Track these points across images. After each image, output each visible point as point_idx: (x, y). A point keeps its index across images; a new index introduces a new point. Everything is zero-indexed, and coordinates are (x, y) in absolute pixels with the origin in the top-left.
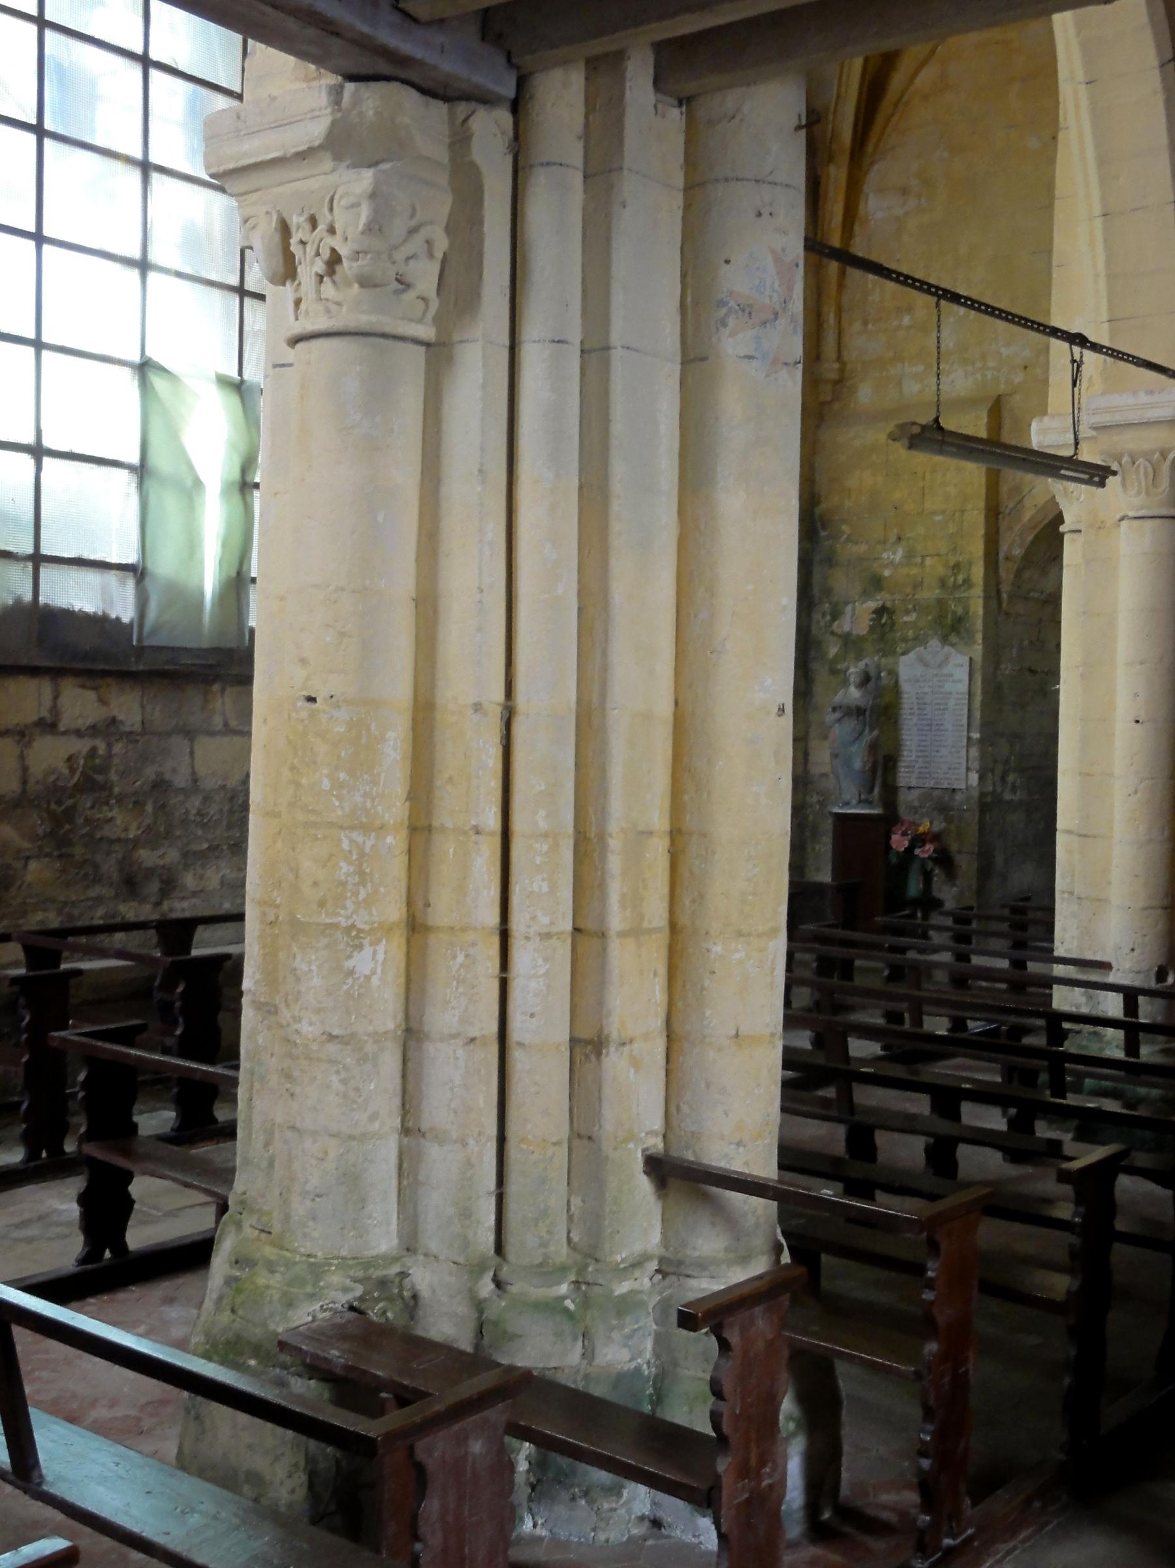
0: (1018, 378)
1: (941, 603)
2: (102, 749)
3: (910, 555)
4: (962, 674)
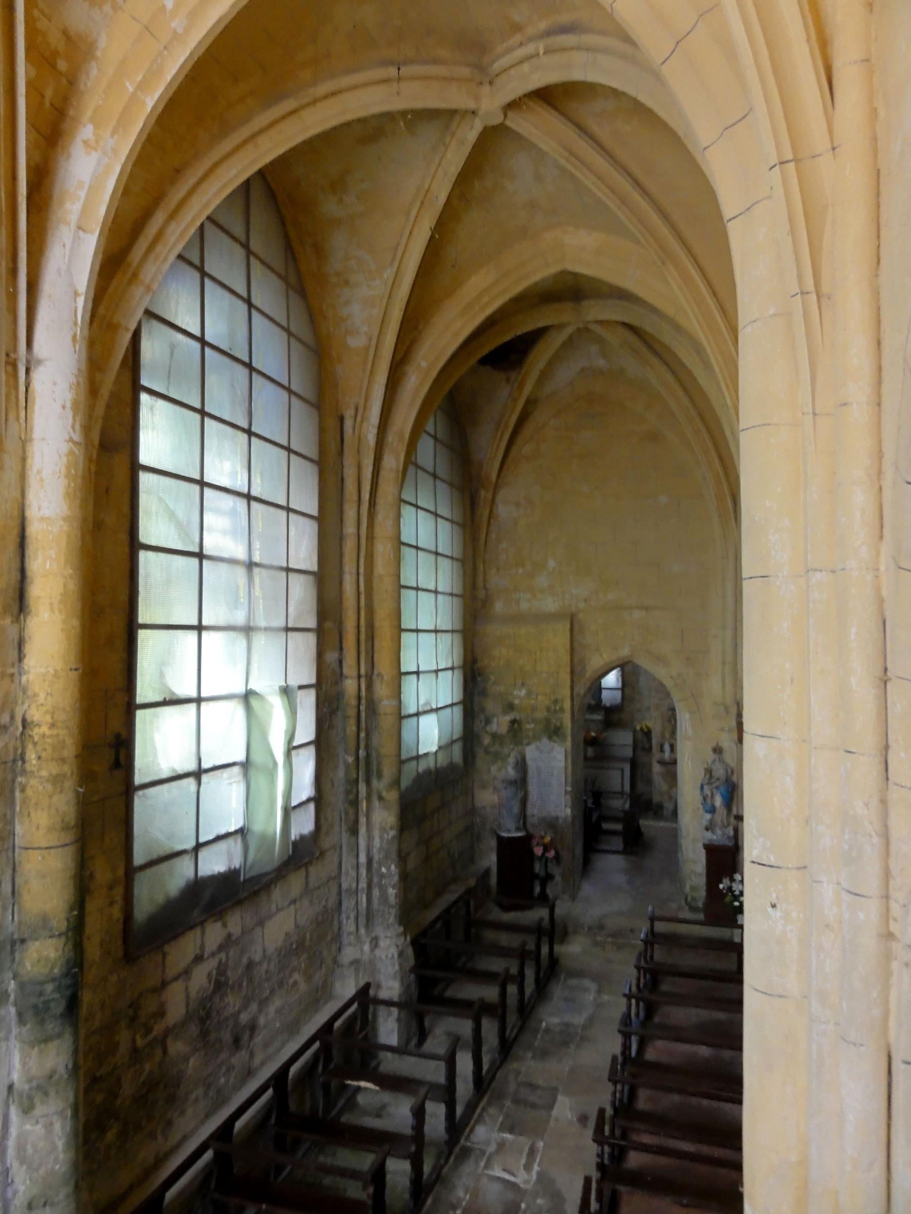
0: (582, 605)
1: (548, 721)
3: (529, 694)
4: (562, 757)
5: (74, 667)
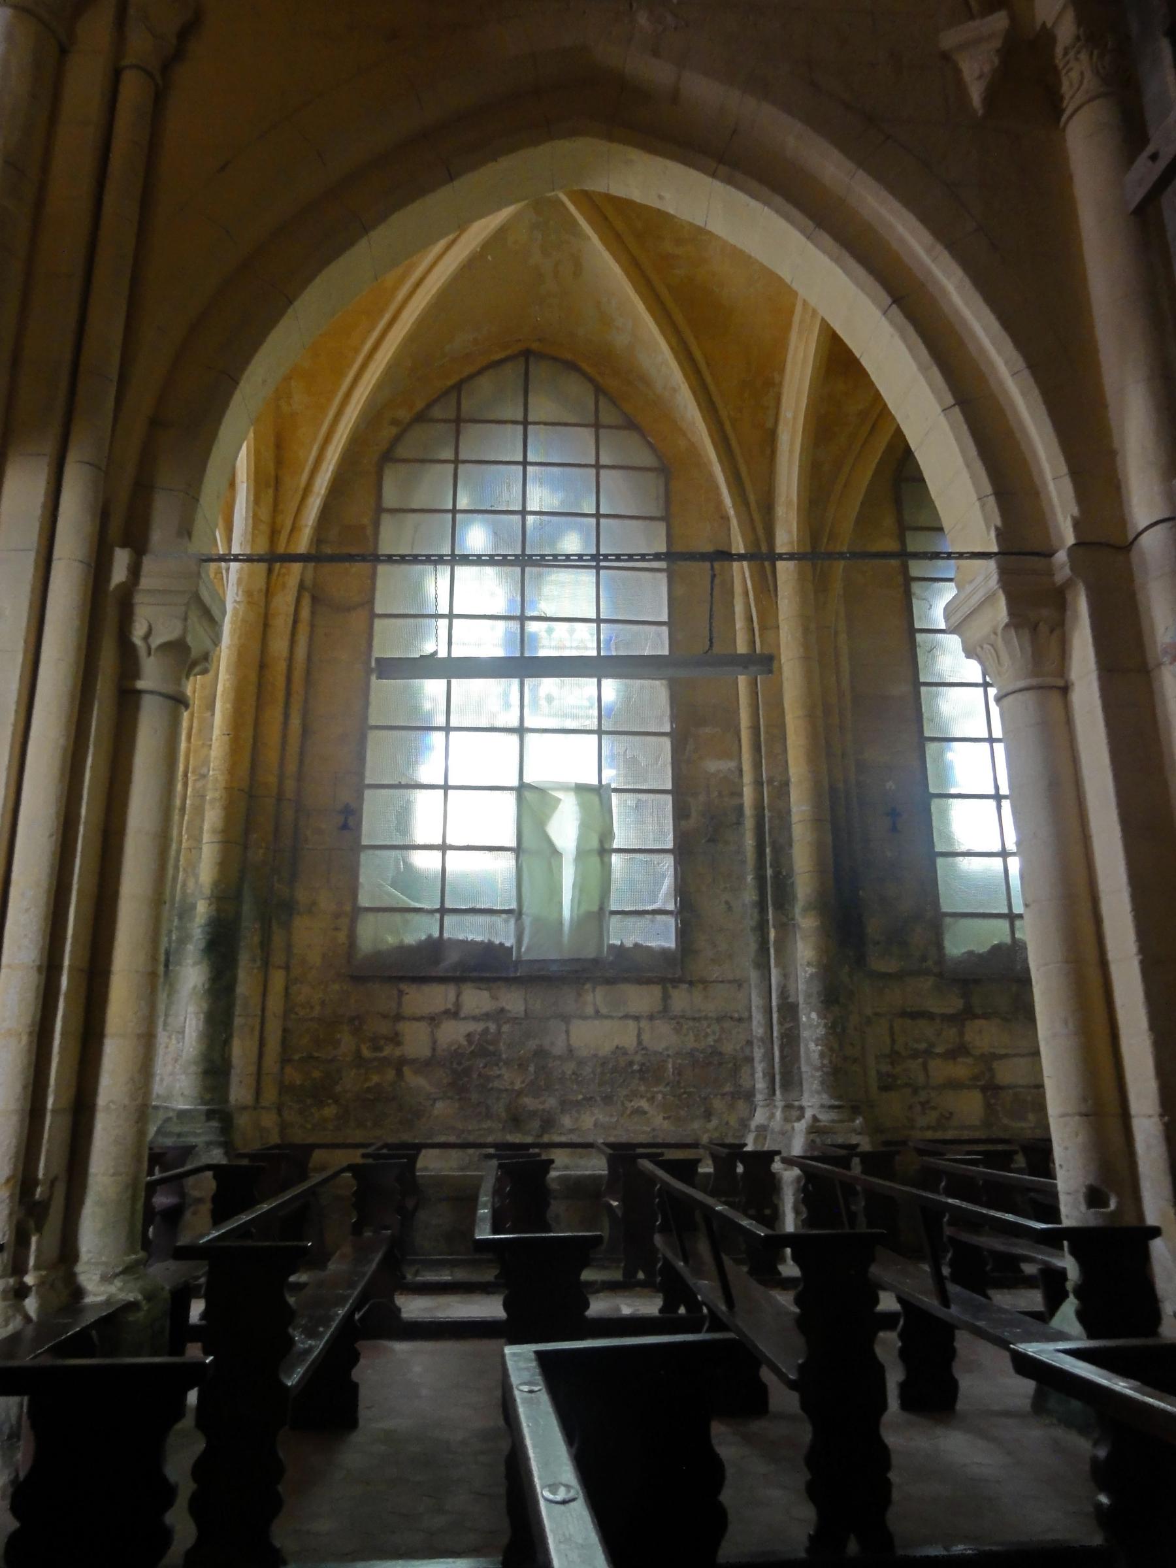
2: (493, 1027)
5: (226, 733)
